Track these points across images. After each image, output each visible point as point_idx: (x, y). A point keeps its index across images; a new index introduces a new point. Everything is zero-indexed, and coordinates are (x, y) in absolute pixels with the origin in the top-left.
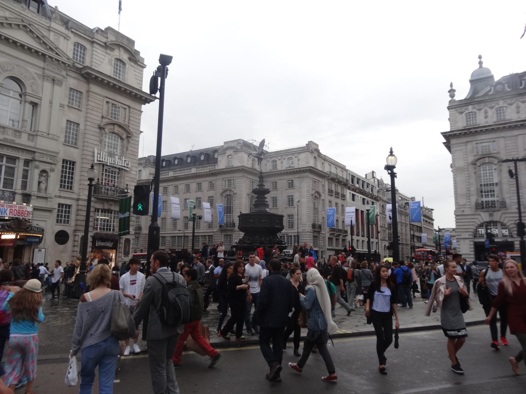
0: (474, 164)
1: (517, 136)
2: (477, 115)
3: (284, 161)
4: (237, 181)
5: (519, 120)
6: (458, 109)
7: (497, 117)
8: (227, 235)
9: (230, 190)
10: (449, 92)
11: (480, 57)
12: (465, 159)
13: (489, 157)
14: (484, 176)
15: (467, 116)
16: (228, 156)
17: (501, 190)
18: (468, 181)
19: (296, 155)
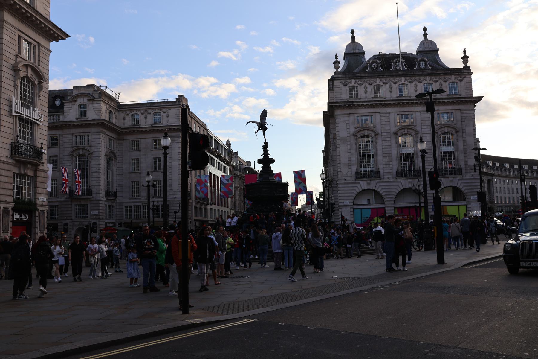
0: (355, 135)
1: (390, 113)
2: (358, 90)
3: (149, 116)
4: (93, 137)
5: (391, 99)
6: (342, 81)
7: (375, 93)
8: (80, 205)
9: (83, 149)
10: (334, 63)
11: (353, 32)
12: (348, 130)
13: (368, 130)
14: (363, 148)
15: (349, 89)
16: (80, 105)
17: (376, 162)
18: (350, 151)
19: (164, 110)
